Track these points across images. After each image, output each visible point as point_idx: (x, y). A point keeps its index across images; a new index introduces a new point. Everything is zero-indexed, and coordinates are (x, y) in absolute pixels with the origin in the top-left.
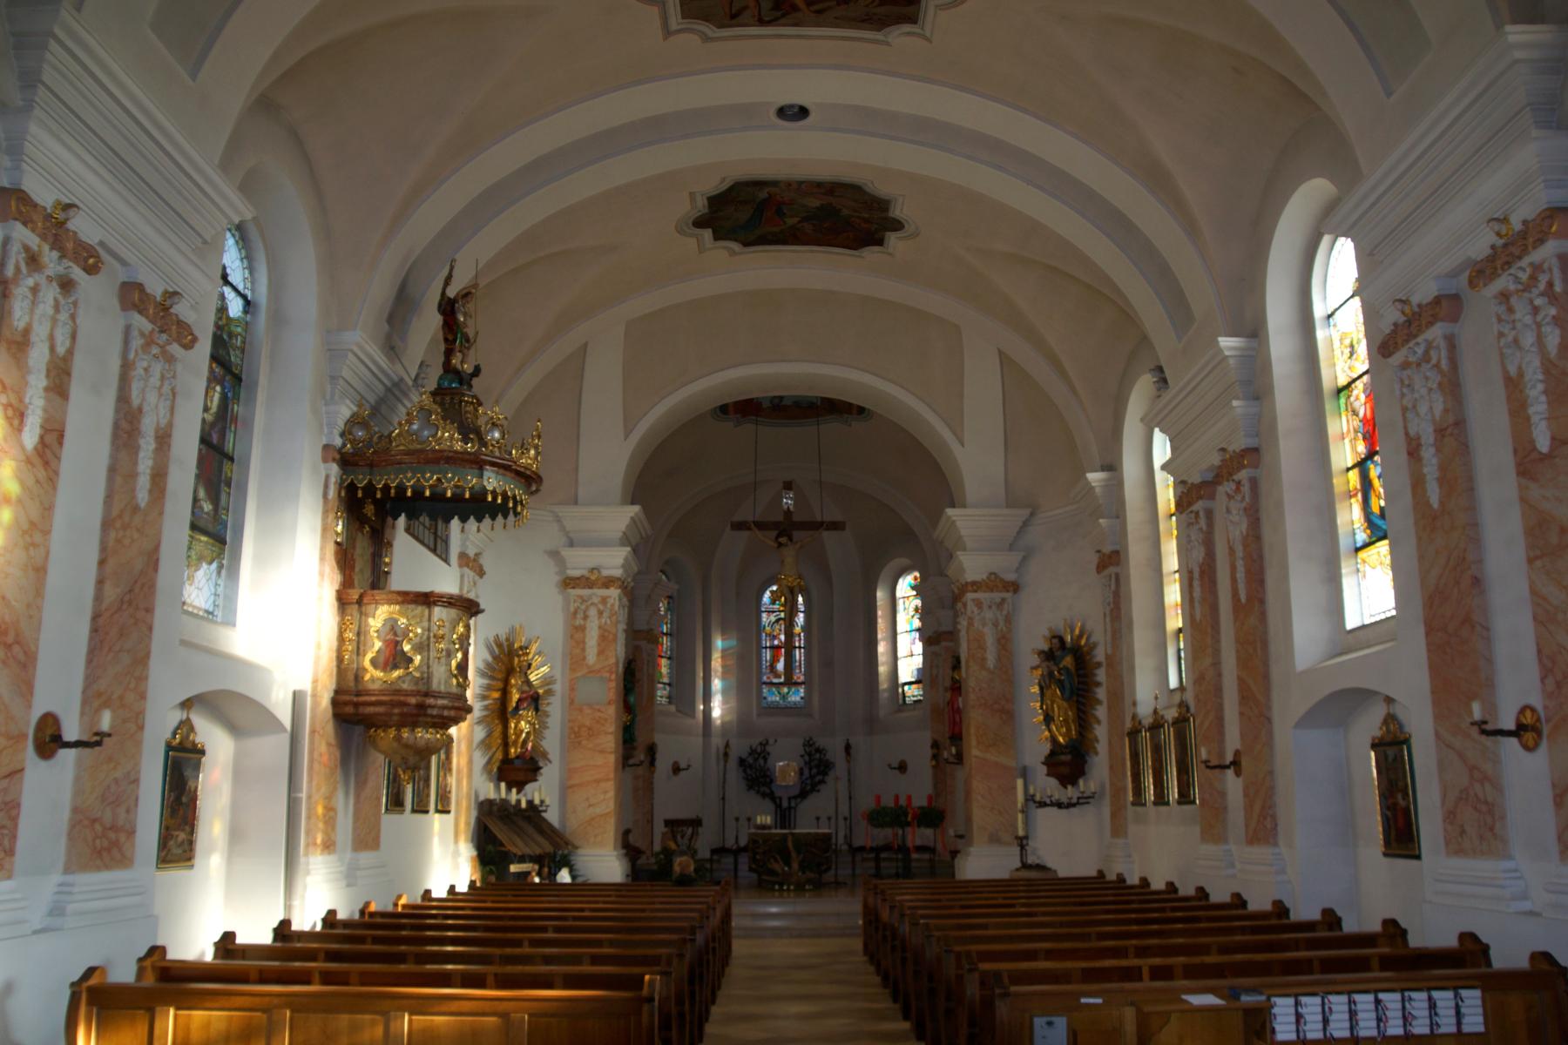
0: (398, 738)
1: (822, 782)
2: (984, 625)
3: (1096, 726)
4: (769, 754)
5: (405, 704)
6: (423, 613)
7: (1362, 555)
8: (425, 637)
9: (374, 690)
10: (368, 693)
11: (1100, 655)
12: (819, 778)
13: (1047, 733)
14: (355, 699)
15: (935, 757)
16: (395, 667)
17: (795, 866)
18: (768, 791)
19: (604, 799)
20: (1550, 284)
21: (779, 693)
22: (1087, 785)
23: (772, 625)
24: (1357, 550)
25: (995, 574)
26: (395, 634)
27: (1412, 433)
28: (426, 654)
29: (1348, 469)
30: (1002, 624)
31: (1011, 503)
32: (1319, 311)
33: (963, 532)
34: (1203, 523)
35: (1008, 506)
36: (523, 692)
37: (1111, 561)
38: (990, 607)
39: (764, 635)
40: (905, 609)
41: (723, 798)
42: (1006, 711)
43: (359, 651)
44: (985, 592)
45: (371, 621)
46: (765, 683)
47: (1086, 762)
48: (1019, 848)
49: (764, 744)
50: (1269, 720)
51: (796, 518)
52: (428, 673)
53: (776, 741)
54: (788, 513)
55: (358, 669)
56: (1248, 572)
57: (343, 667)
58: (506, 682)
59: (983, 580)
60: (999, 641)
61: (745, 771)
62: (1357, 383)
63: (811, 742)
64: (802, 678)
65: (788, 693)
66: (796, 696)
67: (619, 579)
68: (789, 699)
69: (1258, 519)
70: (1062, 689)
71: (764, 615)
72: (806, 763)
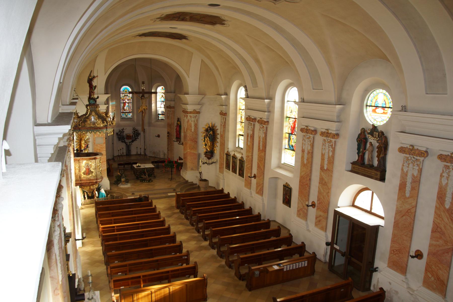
0: (90, 188)
1: (137, 138)
2: (191, 122)
3: (216, 147)
4: (124, 132)
5: (93, 182)
6: (94, 161)
7: (286, 149)
8: (95, 167)
9: (85, 180)
10: (83, 180)
11: (219, 132)
12: (136, 137)
13: (205, 146)
14: (80, 182)
15: (168, 136)
16: (89, 174)
17: (147, 176)
18: (124, 141)
19: (104, 167)
20: (332, 145)
21: (125, 115)
22: (214, 160)
23: (123, 97)
24: (285, 148)
25: (195, 110)
26: (88, 167)
27: (303, 148)
28: (95, 170)
29: (286, 133)
30: (196, 121)
31: (200, 94)
32: (286, 100)
33: (188, 100)
34: (253, 126)
35: (199, 95)
36: (85, 145)
37: (224, 114)
38: (193, 117)
40: (159, 95)
41: (113, 143)
42: (195, 141)
43: (80, 171)
44: (192, 114)
45: (82, 164)
46: (122, 112)
47: (213, 154)
48: (200, 174)
49: (122, 130)
50: (264, 174)
51: (145, 91)
52: (96, 174)
53: (126, 129)
54: (143, 90)
55: (80, 175)
56: (263, 145)
57: (76, 175)
58: (80, 143)
59: (192, 111)
60: (195, 125)
61: (118, 136)
62: (291, 119)
63: (135, 128)
64: (131, 111)
65: (127, 115)
66: (130, 115)
67: (104, 112)
68: (128, 116)
69: (266, 135)
70: (210, 139)
71: (121, 94)
72: (133, 134)
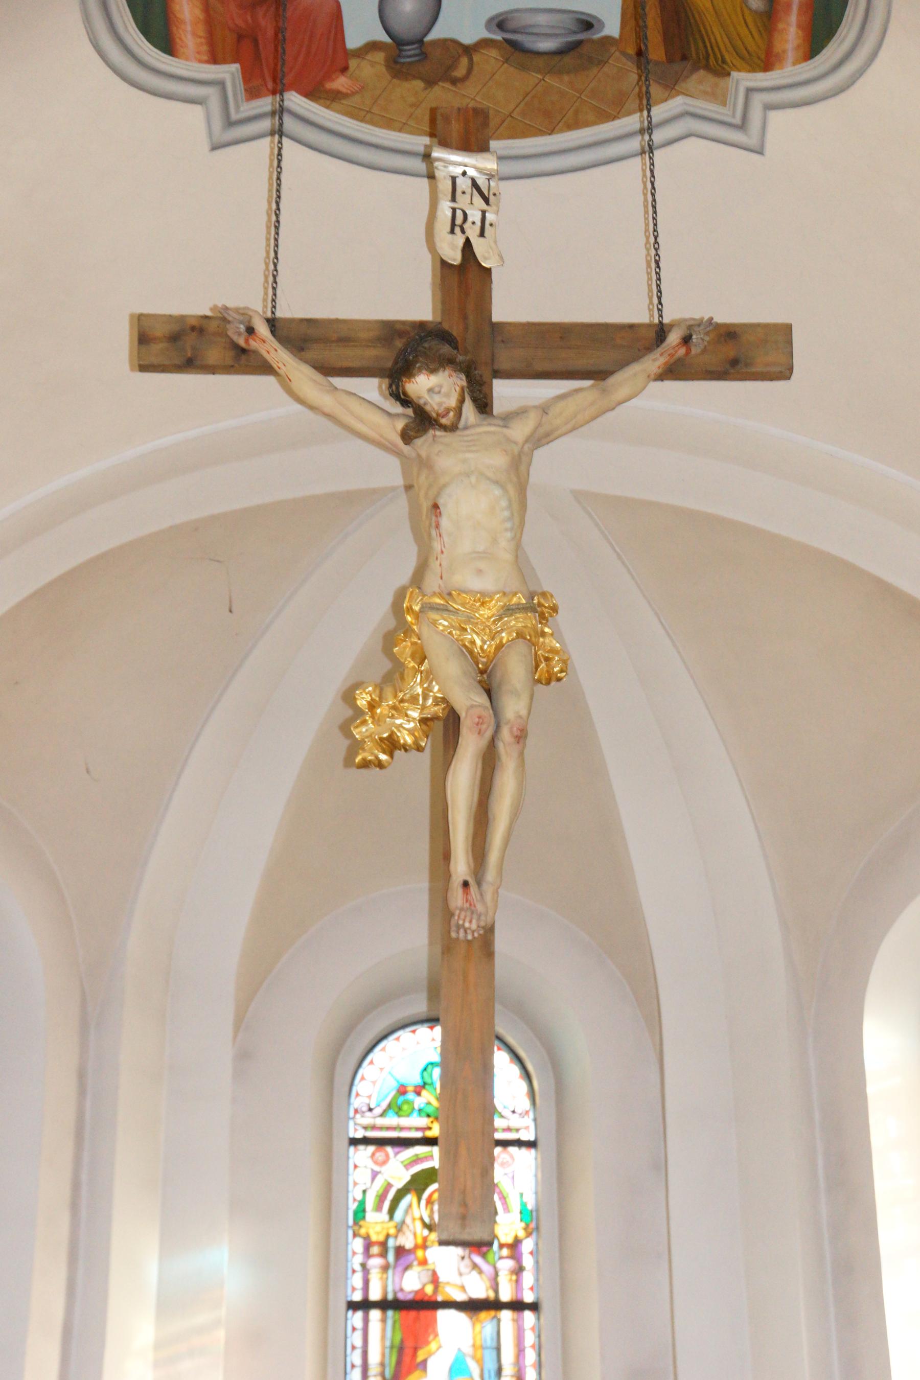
39: (357, 1245)
